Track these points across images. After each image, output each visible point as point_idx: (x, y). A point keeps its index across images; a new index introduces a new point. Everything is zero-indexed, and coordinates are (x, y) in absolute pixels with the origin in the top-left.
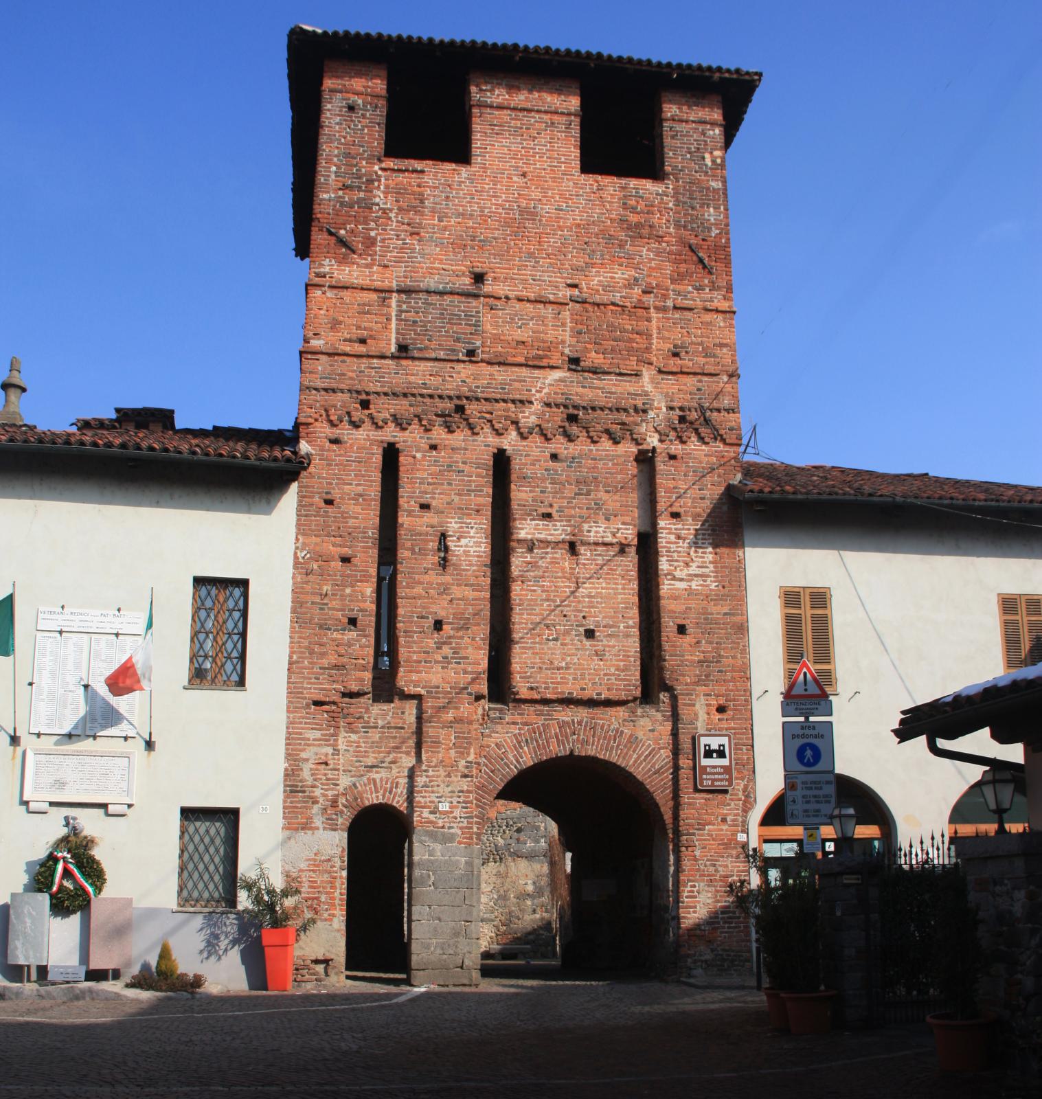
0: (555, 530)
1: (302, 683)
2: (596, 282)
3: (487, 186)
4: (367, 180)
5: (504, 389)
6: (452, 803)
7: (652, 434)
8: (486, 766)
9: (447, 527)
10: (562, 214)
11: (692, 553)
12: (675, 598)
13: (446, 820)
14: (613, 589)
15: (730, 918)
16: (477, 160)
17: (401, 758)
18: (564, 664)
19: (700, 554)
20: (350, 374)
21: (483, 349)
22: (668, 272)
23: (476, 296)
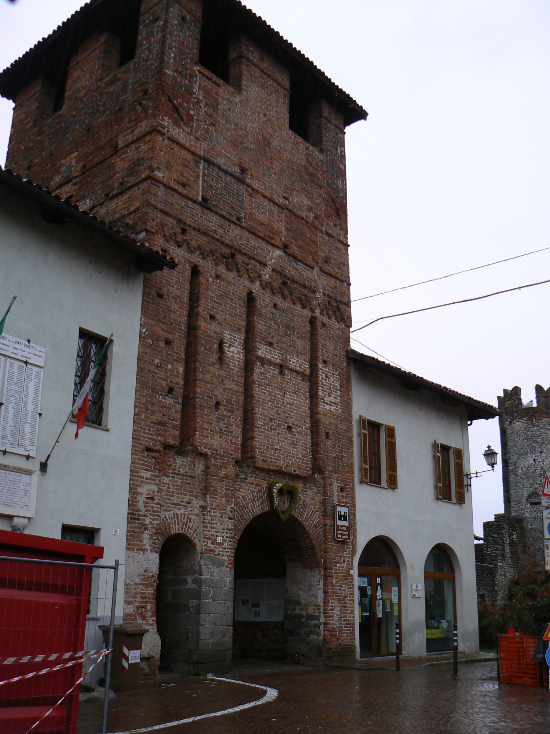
1: (140, 432)
5: (254, 251)
8: (237, 511)
9: (224, 336)
11: (332, 388)
12: (325, 415)
13: (220, 549)
15: (347, 624)
20: (176, 206)
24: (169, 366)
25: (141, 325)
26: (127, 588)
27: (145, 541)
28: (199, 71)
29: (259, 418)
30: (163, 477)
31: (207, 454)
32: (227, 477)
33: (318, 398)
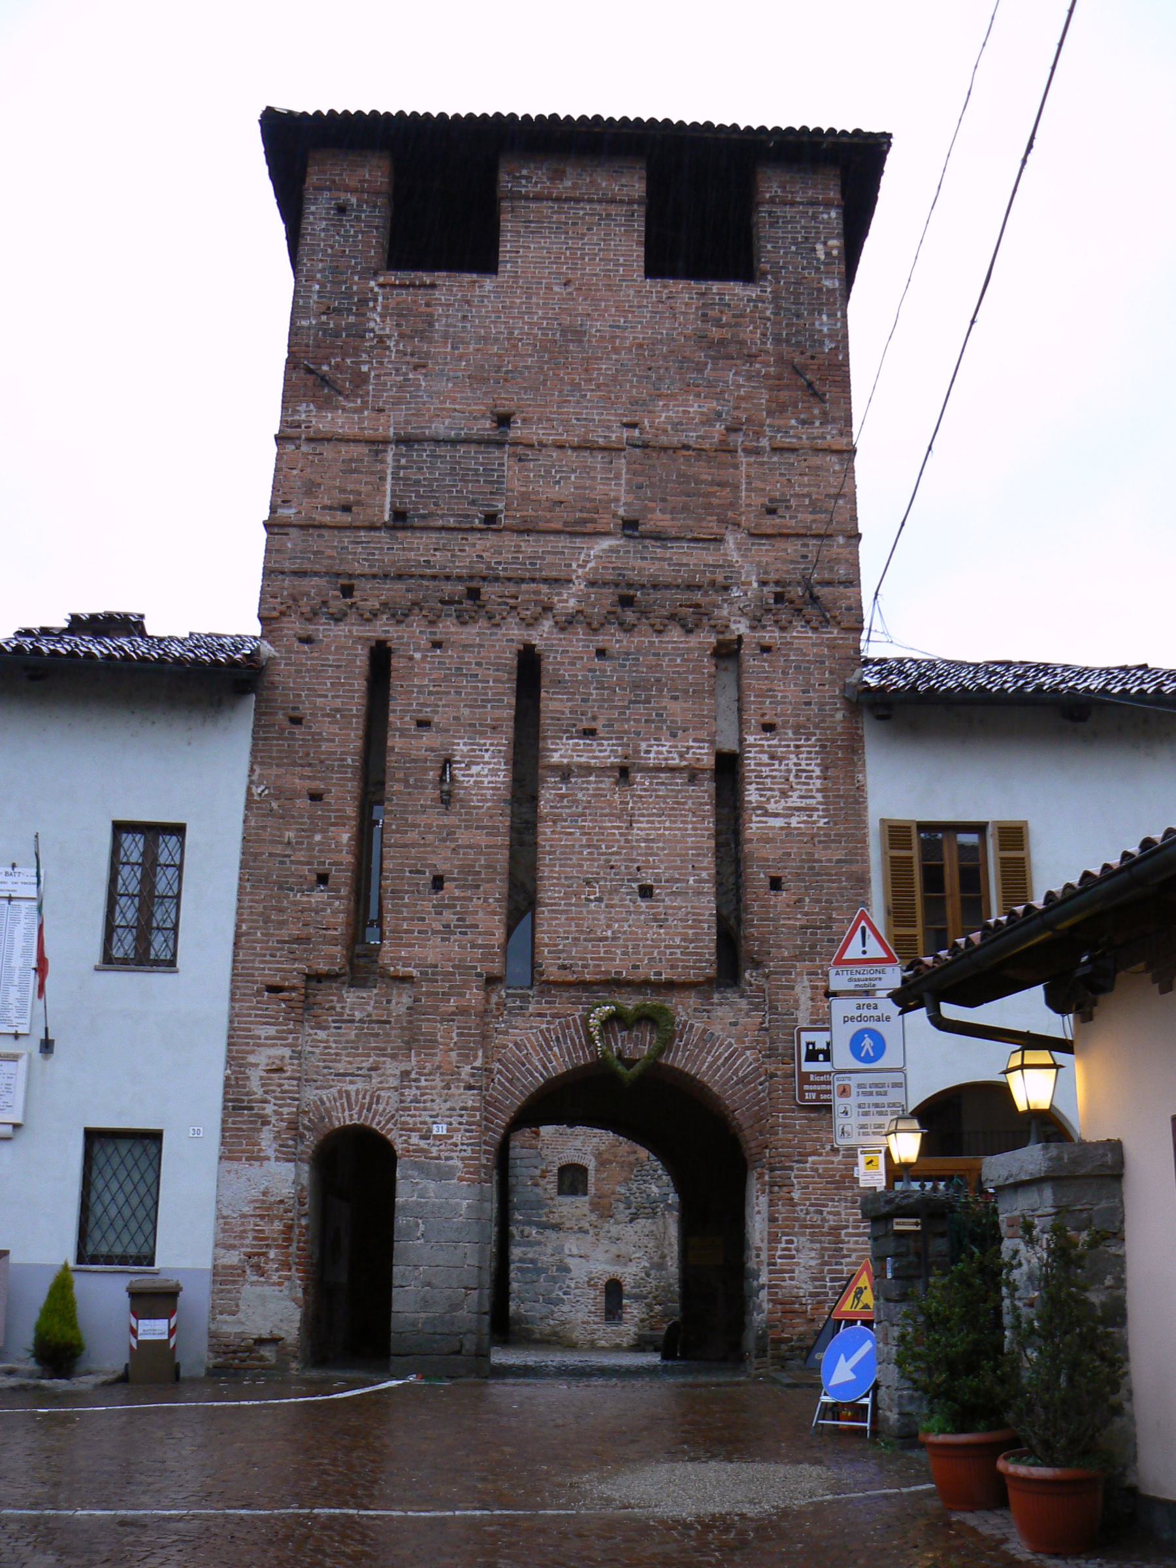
0: (600, 751)
2: (662, 419)
3: (518, 301)
4: (359, 301)
6: (451, 1124)
7: (738, 619)
8: (500, 1072)
10: (618, 332)
11: (792, 779)
12: (768, 840)
13: (442, 1147)
14: (679, 829)
16: (506, 268)
17: (384, 1063)
18: (609, 933)
19: (803, 780)
20: (329, 552)
21: (510, 513)
22: (763, 401)
23: (500, 444)
26: (225, 1224)
29: (553, 885)
31: (412, 977)
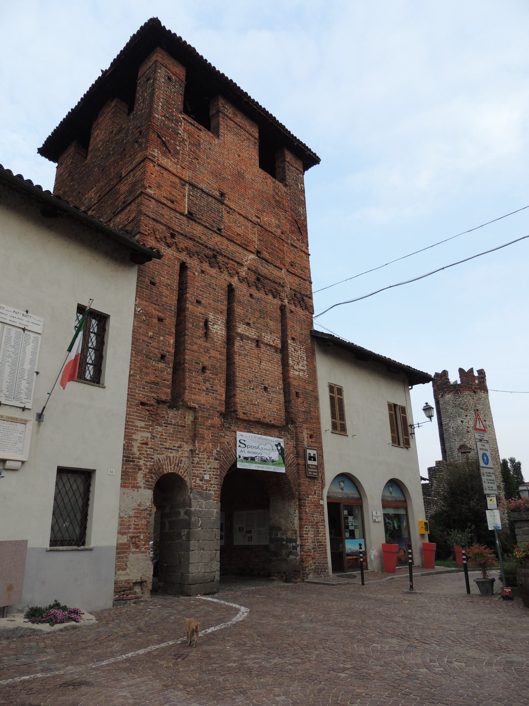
5: (233, 254)
8: (222, 454)
12: (295, 379)
13: (207, 485)
15: (320, 545)
17: (183, 445)
18: (257, 403)
20: (166, 216)
24: (162, 338)
25: (136, 305)
26: (122, 521)
27: (139, 480)
28: (184, 119)
29: (240, 380)
30: (156, 427)
31: (195, 408)
32: (213, 426)
33: (288, 366)
